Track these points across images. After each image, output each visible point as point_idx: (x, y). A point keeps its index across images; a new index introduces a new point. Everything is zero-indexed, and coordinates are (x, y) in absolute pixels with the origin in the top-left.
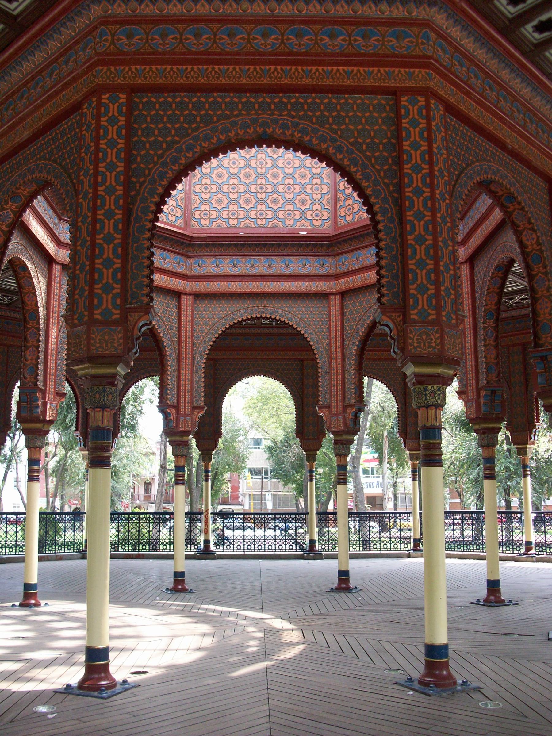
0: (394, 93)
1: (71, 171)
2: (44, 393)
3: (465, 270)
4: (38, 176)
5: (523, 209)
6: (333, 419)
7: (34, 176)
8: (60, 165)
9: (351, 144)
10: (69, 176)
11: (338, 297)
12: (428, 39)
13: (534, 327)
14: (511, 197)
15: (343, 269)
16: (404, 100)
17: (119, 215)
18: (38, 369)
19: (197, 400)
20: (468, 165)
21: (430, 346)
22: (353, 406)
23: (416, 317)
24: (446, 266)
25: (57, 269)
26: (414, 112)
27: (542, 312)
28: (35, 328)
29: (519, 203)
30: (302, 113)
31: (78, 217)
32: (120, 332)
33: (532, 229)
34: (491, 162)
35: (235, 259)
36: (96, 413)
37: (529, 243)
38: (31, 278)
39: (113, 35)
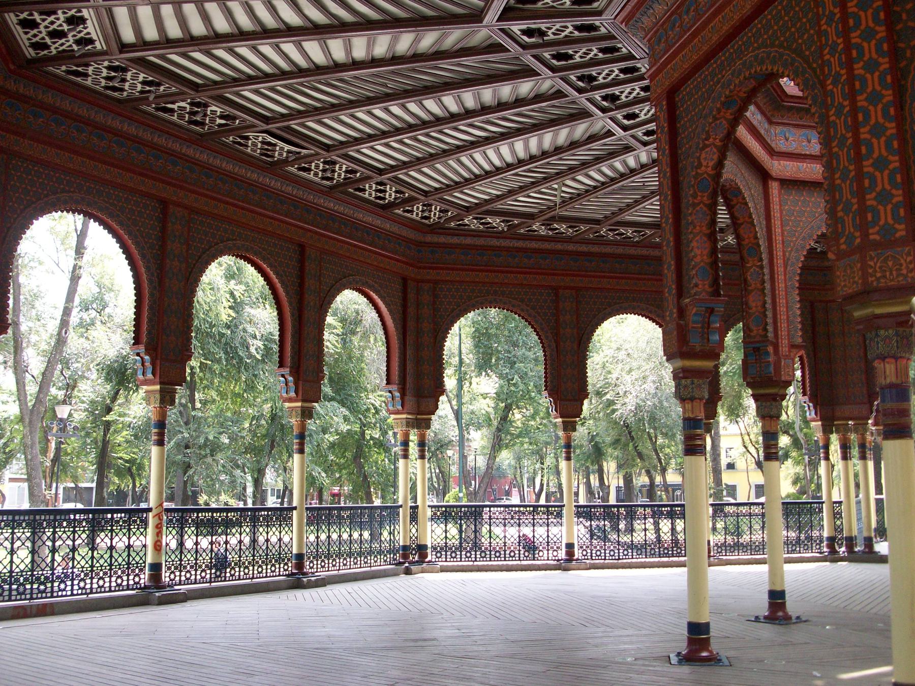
1: (807, 53)
2: (776, 347)
4: (758, 69)
7: (753, 71)
17: (888, 96)
18: (766, 316)
25: (774, 187)
28: (757, 266)
32: (908, 254)
36: (887, 366)
38: (746, 204)
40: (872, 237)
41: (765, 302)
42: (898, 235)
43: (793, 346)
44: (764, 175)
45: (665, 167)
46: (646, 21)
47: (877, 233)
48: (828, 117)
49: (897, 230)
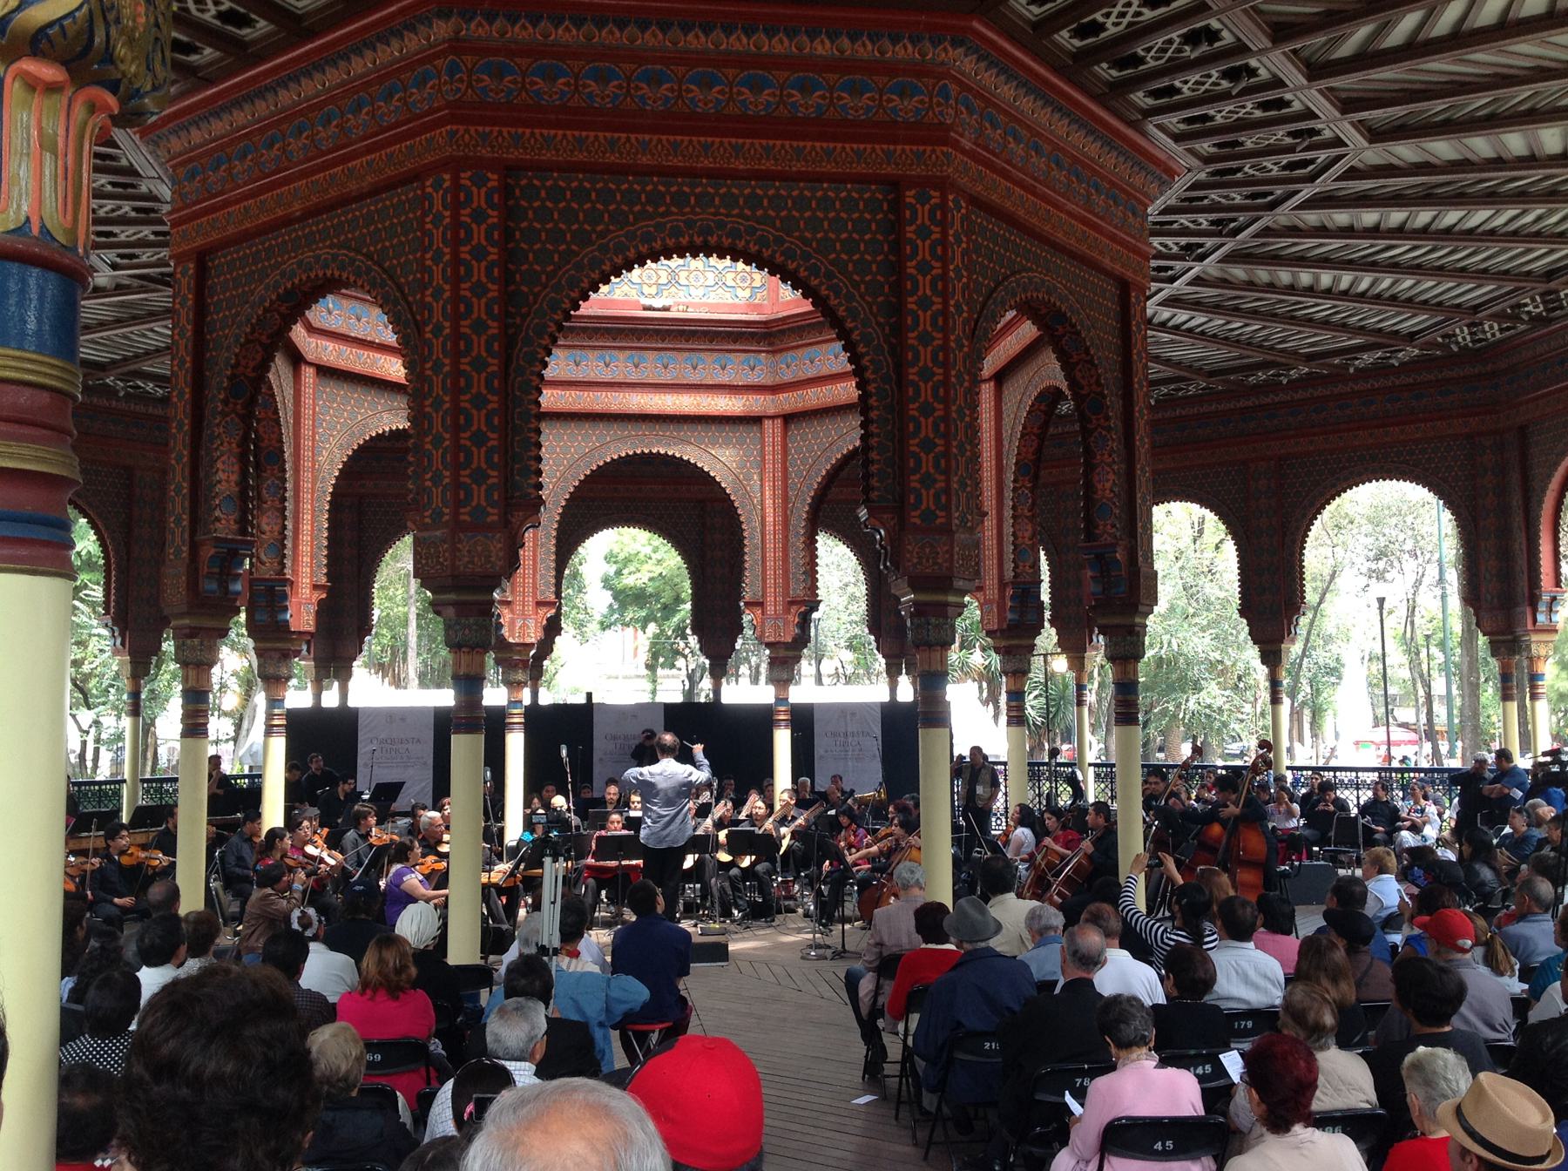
0: (895, 185)
3: (987, 390)
5: (1078, 333)
6: (769, 623)
7: (329, 273)
8: (380, 266)
9: (831, 263)
10: (399, 287)
11: (779, 422)
12: (947, 98)
13: (1087, 508)
14: (1061, 317)
15: (788, 377)
16: (910, 196)
17: (494, 365)
18: (284, 546)
19: (543, 593)
20: (998, 284)
21: (935, 563)
22: (802, 603)
23: (918, 521)
24: (960, 410)
25: (308, 374)
26: (923, 212)
27: (1100, 486)
29: (1074, 326)
30: (759, 213)
31: (424, 361)
33: (1091, 362)
34: (1031, 270)
35: (607, 355)
37: (1084, 382)
38: (273, 396)
39: (470, 72)
40: (462, 517)
41: (284, 527)
42: (489, 520)
43: (315, 587)
44: (297, 359)
45: (182, 352)
46: (176, 144)
47: (469, 514)
48: (423, 370)
49: (489, 514)
